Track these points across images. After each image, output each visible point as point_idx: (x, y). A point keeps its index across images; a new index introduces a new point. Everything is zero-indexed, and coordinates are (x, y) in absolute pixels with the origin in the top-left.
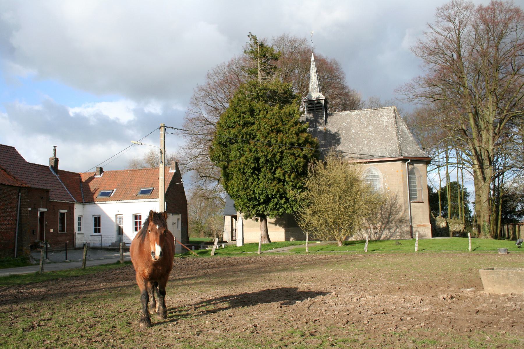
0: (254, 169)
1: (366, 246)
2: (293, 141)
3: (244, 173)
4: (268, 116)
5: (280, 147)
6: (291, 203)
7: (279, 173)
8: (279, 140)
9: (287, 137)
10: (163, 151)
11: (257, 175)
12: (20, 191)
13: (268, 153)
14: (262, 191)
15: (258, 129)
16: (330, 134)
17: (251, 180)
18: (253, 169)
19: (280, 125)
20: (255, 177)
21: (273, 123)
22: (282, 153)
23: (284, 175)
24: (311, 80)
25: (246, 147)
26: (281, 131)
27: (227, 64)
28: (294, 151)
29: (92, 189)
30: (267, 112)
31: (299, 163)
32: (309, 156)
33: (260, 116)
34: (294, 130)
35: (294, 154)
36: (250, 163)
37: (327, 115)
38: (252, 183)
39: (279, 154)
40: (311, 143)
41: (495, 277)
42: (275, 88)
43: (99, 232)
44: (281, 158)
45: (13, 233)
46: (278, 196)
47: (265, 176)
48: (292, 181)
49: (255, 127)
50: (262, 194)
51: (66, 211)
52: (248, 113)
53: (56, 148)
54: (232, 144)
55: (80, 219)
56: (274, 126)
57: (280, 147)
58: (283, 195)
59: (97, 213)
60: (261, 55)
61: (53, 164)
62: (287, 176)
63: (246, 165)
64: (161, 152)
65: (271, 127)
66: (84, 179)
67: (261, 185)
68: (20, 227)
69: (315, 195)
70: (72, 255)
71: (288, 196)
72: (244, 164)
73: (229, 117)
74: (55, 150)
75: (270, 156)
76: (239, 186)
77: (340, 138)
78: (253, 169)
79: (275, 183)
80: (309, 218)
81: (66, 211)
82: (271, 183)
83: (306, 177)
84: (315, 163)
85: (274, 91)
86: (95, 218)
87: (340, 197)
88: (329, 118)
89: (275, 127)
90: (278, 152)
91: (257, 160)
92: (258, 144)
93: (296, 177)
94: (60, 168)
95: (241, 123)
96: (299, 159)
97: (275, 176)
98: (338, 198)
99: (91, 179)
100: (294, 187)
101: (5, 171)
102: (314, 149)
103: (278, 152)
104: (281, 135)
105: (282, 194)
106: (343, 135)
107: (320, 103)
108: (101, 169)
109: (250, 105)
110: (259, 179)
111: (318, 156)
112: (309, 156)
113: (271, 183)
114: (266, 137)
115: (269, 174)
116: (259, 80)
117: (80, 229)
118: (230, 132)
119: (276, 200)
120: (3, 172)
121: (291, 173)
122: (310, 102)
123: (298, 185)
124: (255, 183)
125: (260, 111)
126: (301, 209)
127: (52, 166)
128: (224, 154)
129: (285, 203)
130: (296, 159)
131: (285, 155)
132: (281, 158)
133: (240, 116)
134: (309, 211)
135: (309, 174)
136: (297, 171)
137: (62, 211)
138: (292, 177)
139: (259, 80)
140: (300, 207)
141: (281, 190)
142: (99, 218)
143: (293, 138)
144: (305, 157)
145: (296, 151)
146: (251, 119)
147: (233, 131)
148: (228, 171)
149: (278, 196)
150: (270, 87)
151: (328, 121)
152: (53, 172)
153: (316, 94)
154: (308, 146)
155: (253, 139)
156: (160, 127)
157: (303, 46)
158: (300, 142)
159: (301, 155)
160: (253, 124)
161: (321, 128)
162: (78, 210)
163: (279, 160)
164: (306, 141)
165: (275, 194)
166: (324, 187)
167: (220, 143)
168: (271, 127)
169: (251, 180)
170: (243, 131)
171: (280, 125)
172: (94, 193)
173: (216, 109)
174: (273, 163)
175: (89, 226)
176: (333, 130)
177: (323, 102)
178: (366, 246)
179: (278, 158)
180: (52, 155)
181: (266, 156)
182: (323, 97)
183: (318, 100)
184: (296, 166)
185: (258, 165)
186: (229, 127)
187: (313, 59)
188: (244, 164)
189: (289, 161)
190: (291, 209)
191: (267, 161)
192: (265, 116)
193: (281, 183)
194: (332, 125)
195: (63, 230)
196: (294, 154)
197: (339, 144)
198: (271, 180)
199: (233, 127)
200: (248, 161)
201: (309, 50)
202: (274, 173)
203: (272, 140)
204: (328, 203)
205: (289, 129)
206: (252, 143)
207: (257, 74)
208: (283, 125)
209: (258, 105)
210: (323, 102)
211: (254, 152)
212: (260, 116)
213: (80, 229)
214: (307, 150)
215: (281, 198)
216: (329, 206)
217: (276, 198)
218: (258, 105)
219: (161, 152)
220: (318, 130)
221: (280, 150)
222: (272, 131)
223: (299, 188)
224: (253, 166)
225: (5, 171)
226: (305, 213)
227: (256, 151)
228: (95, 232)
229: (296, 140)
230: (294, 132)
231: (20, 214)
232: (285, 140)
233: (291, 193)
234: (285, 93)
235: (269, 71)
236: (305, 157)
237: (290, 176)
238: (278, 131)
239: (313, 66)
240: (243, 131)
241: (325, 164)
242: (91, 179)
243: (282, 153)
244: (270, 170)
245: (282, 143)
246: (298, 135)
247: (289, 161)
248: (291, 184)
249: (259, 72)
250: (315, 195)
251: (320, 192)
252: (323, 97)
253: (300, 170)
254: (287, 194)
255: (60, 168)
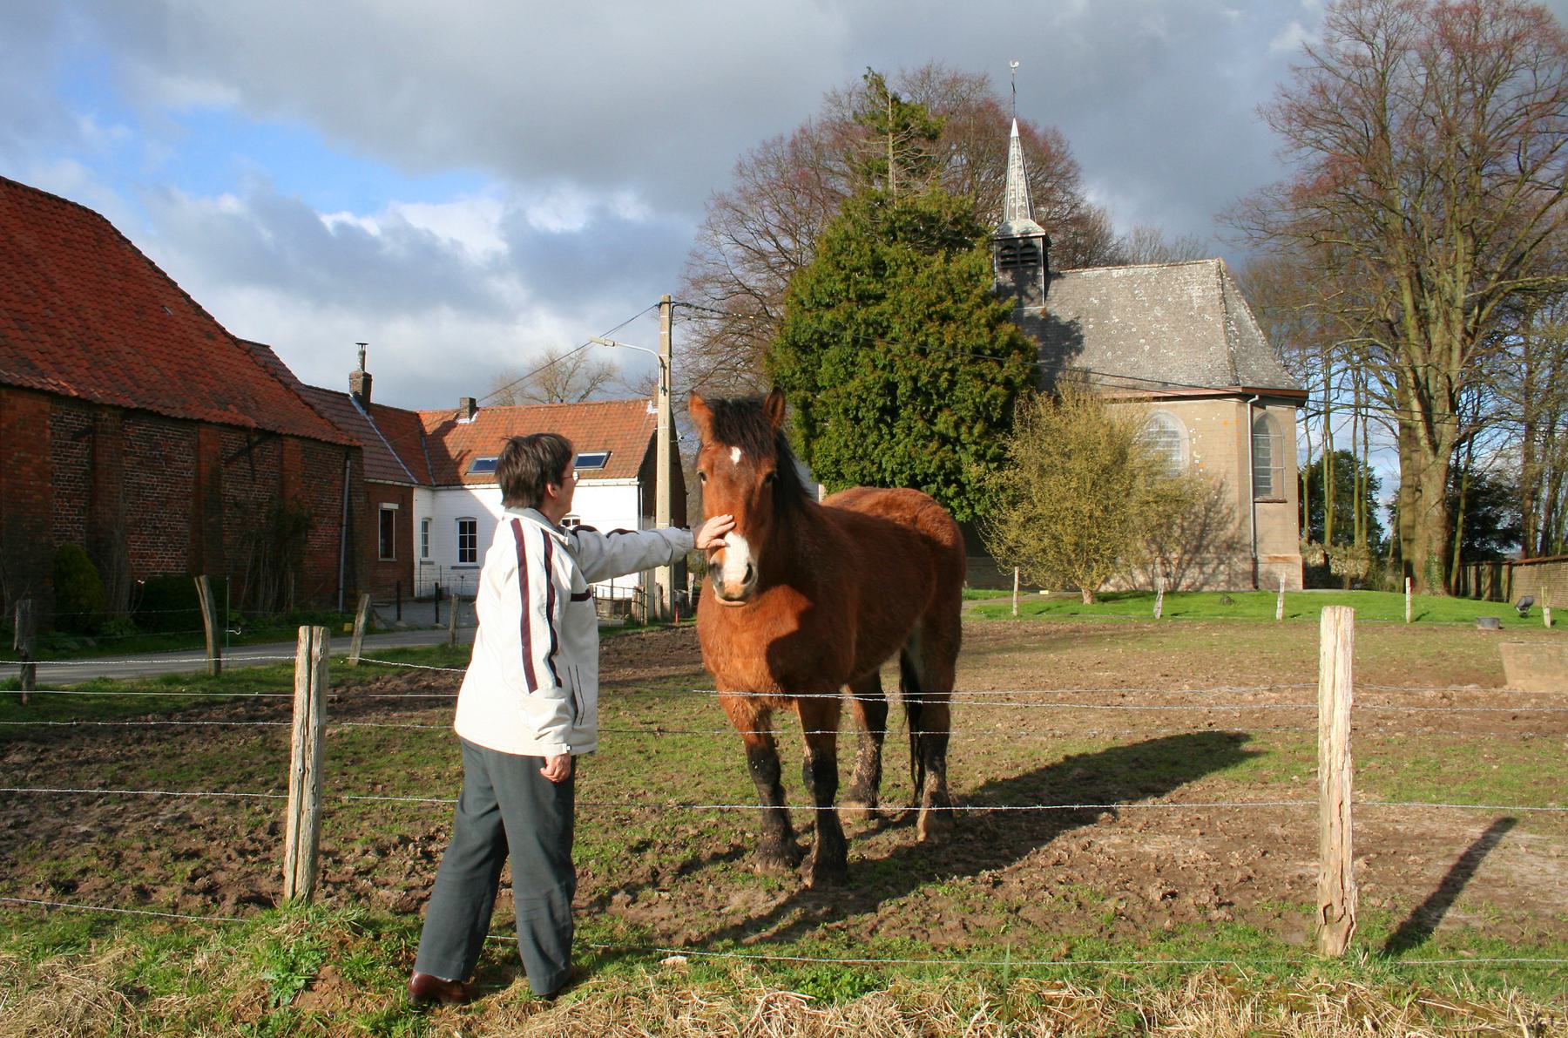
0: (883, 410)
1: (1160, 604)
2: (980, 342)
3: (857, 420)
4: (921, 278)
5: (948, 359)
6: (971, 496)
7: (943, 423)
8: (948, 340)
9: (967, 333)
10: (666, 362)
11: (890, 426)
12: (347, 458)
13: (919, 372)
14: (902, 464)
15: (896, 313)
16: (1057, 325)
17: (873, 437)
18: (879, 409)
19: (949, 303)
20: (885, 430)
21: (933, 297)
22: (953, 371)
23: (957, 426)
24: (1010, 188)
25: (862, 355)
26: (952, 318)
27: (789, 140)
28: (983, 367)
29: (453, 453)
30: (916, 269)
31: (994, 397)
32: (1018, 380)
33: (899, 280)
34: (982, 315)
35: (981, 376)
36: (873, 396)
37: (1049, 277)
38: (876, 445)
39: (946, 375)
40: (1023, 349)
41: (1534, 659)
42: (934, 209)
43: (473, 558)
44: (952, 384)
45: (333, 555)
46: (939, 479)
47: (910, 428)
48: (975, 443)
49: (886, 306)
50: (901, 472)
51: (394, 506)
52: (867, 271)
53: (367, 348)
54: (825, 346)
55: (425, 525)
56: (934, 305)
57: (948, 359)
58: (952, 475)
59: (467, 513)
60: (897, 125)
61: (359, 389)
62: (963, 429)
63: (864, 401)
64: (663, 366)
65: (929, 306)
66: (430, 426)
67: (899, 450)
68: (351, 544)
69: (1034, 479)
70: (411, 614)
71: (963, 479)
72: (859, 397)
73: (819, 282)
74: (363, 354)
75: (924, 378)
76: (843, 451)
77: (1081, 337)
78: (879, 409)
79: (933, 445)
80: (1012, 535)
81: (394, 506)
82: (924, 446)
83: (1010, 432)
84: (1031, 399)
85: (932, 219)
86: (463, 526)
87: (1093, 484)
88: (1054, 283)
89: (938, 308)
90: (943, 370)
91: (890, 388)
92: (896, 349)
93: (985, 434)
94: (376, 398)
95: (852, 295)
96: (994, 389)
97: (935, 429)
98: (1089, 485)
99: (449, 426)
100: (980, 457)
101: (312, 408)
102: (1029, 365)
103: (943, 370)
104: (953, 326)
105: (951, 473)
106: (1088, 327)
107: (1031, 246)
108: (472, 401)
109: (873, 251)
110: (893, 436)
111: (1040, 381)
112: (1018, 380)
113: (924, 446)
114: (915, 332)
115: (920, 424)
116: (892, 187)
117: (425, 552)
118: (820, 318)
119: (933, 487)
120: (307, 410)
121: (974, 421)
122: (1008, 242)
123: (990, 452)
124: (884, 445)
125: (899, 267)
126: (994, 512)
127: (356, 394)
128: (804, 371)
129: (957, 494)
130: (987, 389)
131: (961, 376)
132: (952, 384)
133: (847, 278)
134: (1016, 516)
135: (1017, 427)
136: (988, 419)
137: (387, 506)
138: (976, 431)
139: (892, 187)
140: (994, 505)
141: (948, 465)
142: (473, 525)
143: (979, 335)
144: (1008, 383)
145: (988, 367)
146: (875, 287)
147: (828, 316)
148: (815, 415)
149: (939, 479)
150: (921, 206)
151: (1051, 292)
152: (360, 410)
153: (1020, 224)
154: (1016, 356)
155: (882, 336)
156: (660, 306)
157: (977, 98)
158: (997, 345)
159: (1000, 378)
160: (880, 298)
161: (1032, 309)
162: (422, 504)
163: (946, 391)
164: (1012, 343)
165: (934, 474)
166: (1057, 459)
167: (795, 344)
168: (929, 306)
169: (873, 437)
170: (859, 317)
171: (949, 303)
172: (460, 463)
173: (762, 255)
174: (928, 397)
175: (446, 547)
176: (1065, 315)
177: (1039, 243)
178: (1160, 604)
179: (943, 384)
180: (355, 366)
181: (915, 379)
182: (1041, 231)
183: (1027, 239)
184: (986, 406)
185: (894, 398)
186: (819, 304)
187: (1015, 132)
188: (859, 397)
189: (970, 392)
190: (968, 511)
191: (916, 391)
192: (912, 281)
193: (949, 447)
194: (1061, 303)
195: (387, 554)
196: (981, 376)
197: (1079, 352)
198: (924, 437)
199: (828, 306)
200: (868, 390)
201: (990, 108)
202: (931, 422)
203: (931, 340)
204: (1065, 499)
205: (971, 314)
206: (880, 346)
207: (886, 172)
208: (955, 302)
209: (893, 252)
210: (1039, 243)
211: (884, 368)
212: (899, 280)
213: (425, 552)
214: (1012, 367)
215: (947, 483)
216: (1068, 504)
217: (933, 482)
218: (893, 252)
219: (663, 366)
220: (1026, 314)
221: (949, 365)
222: (930, 317)
223: (992, 460)
224: (880, 403)
225: (312, 408)
226: (1005, 522)
227: (891, 366)
228: (463, 559)
229: (987, 340)
230: (983, 321)
231: (350, 510)
232: (962, 340)
233: (972, 471)
234: (956, 222)
235: (918, 168)
236: (1008, 383)
237: (971, 428)
238: (945, 318)
239: (1015, 151)
240: (859, 317)
241: (1057, 401)
242: (449, 426)
243: (953, 371)
244: (923, 413)
245: (954, 346)
246: (992, 329)
247: (970, 392)
248: (973, 448)
249: (891, 168)
250: (1034, 479)
251: (1043, 472)
252: (1041, 231)
253: (996, 415)
254: (961, 473)
255: (376, 398)
